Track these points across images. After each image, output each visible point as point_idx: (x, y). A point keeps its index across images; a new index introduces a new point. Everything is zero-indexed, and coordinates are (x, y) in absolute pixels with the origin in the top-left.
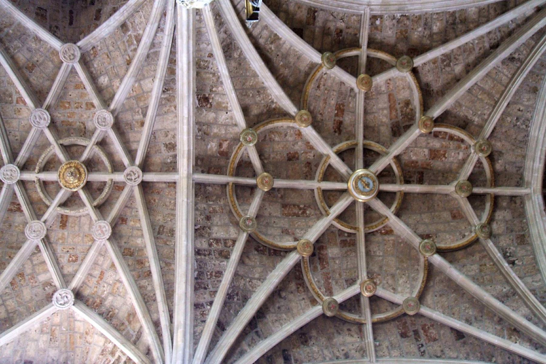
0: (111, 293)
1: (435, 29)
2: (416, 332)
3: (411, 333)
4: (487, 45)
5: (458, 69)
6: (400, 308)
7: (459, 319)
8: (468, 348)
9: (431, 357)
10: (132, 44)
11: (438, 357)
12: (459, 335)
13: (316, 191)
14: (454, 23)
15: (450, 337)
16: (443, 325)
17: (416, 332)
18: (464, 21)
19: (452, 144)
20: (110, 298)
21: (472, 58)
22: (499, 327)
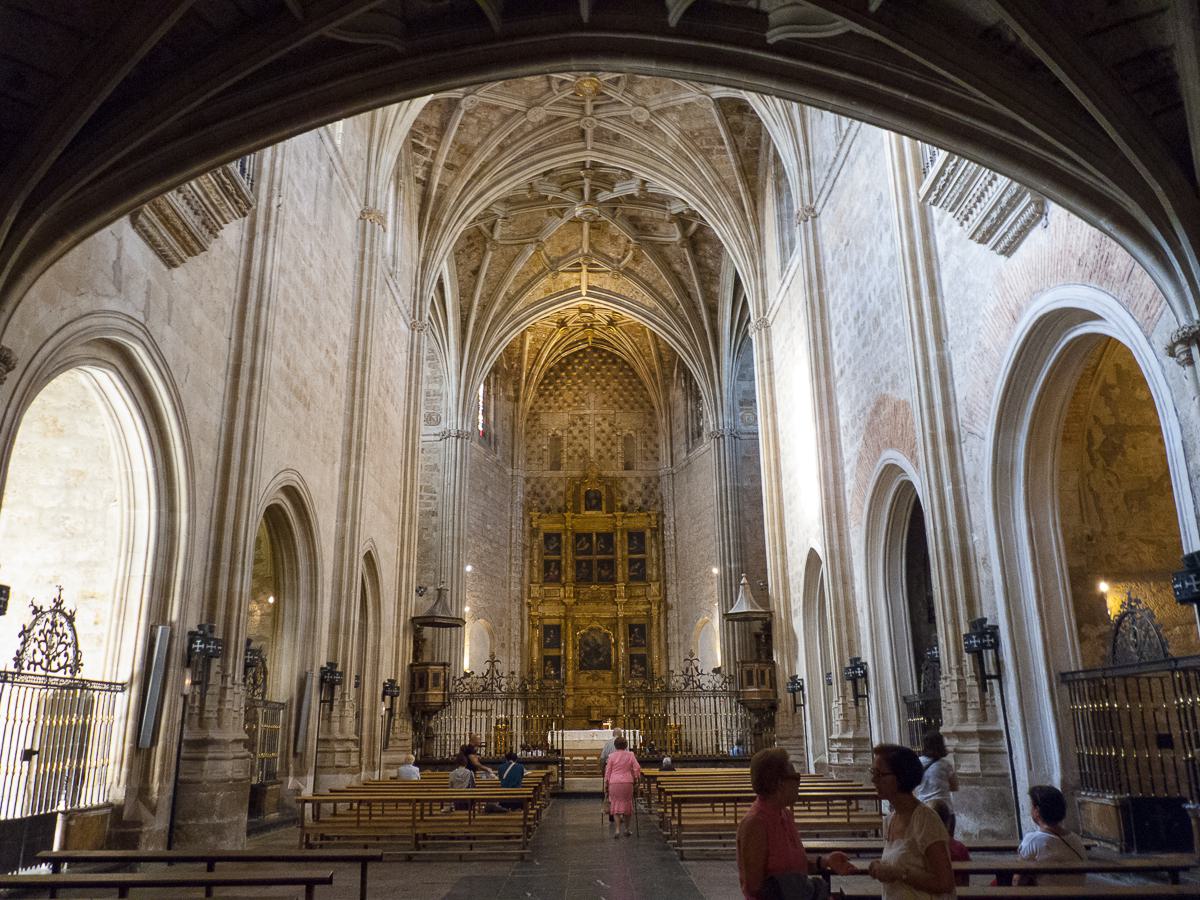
0: (479, 121)
1: (709, 261)
2: (472, 245)
3: (471, 241)
4: (690, 291)
5: (678, 267)
6: (490, 235)
7: (488, 270)
8: (466, 279)
9: (456, 259)
10: (707, 144)
11: (457, 264)
12: (476, 272)
13: (580, 182)
14: (711, 274)
15: (473, 266)
16: (481, 261)
17: (472, 245)
18: (711, 281)
19: (621, 250)
20: (475, 121)
21: (683, 278)
22: (484, 296)
